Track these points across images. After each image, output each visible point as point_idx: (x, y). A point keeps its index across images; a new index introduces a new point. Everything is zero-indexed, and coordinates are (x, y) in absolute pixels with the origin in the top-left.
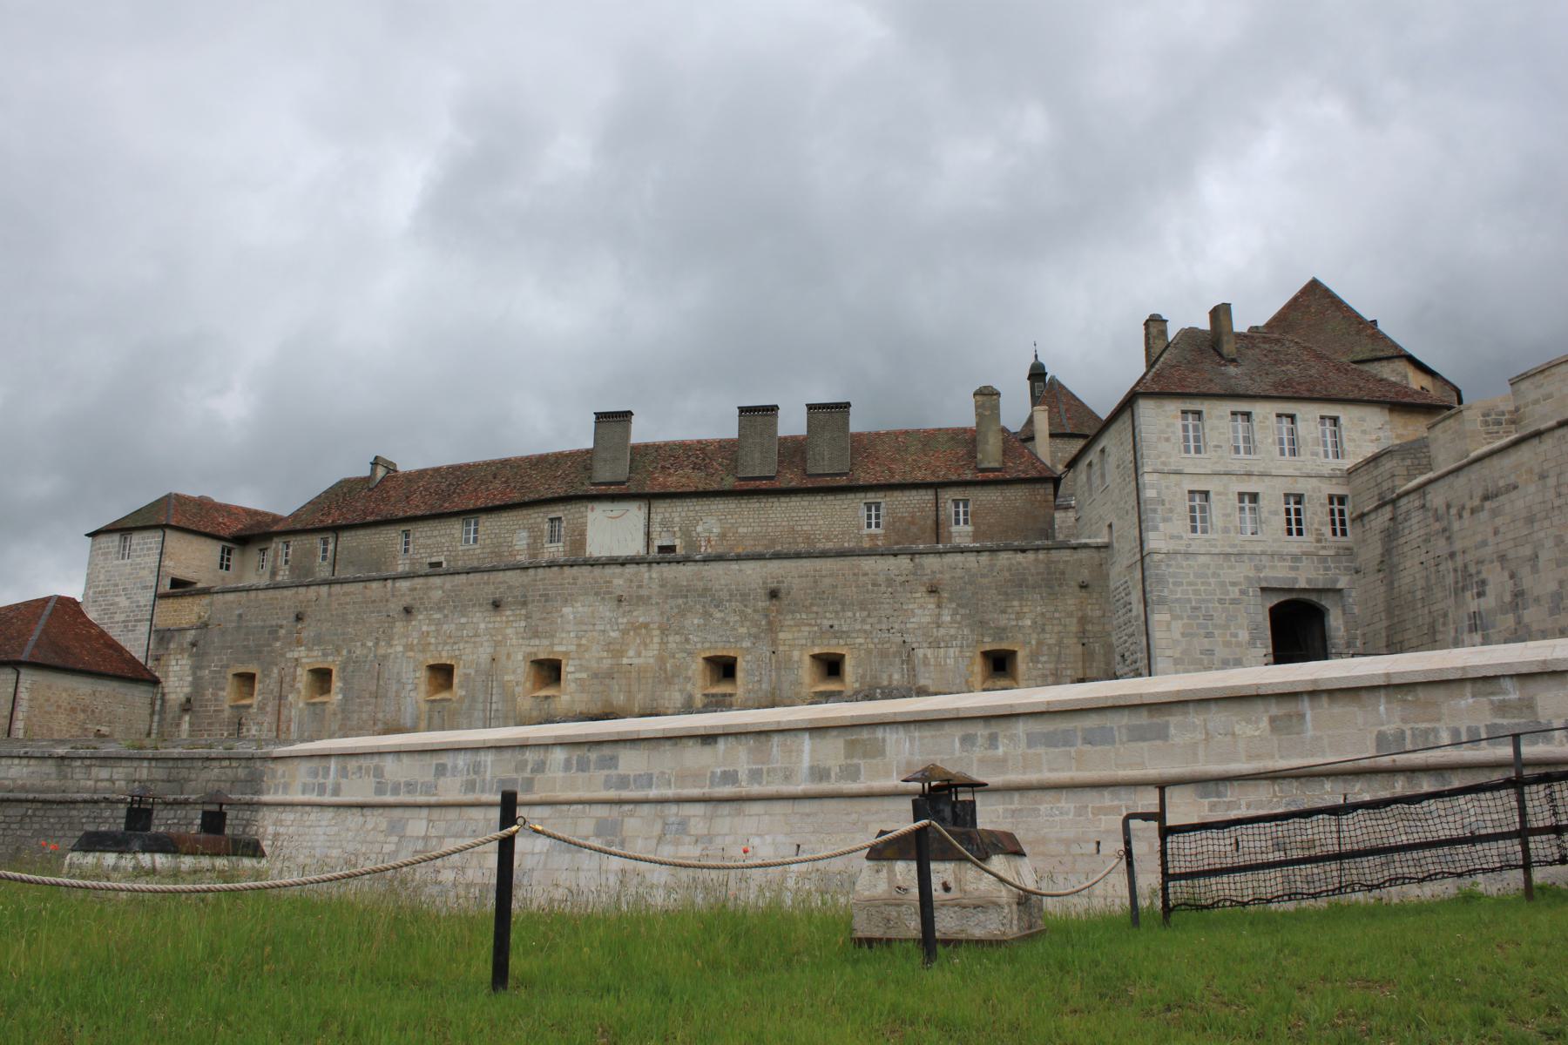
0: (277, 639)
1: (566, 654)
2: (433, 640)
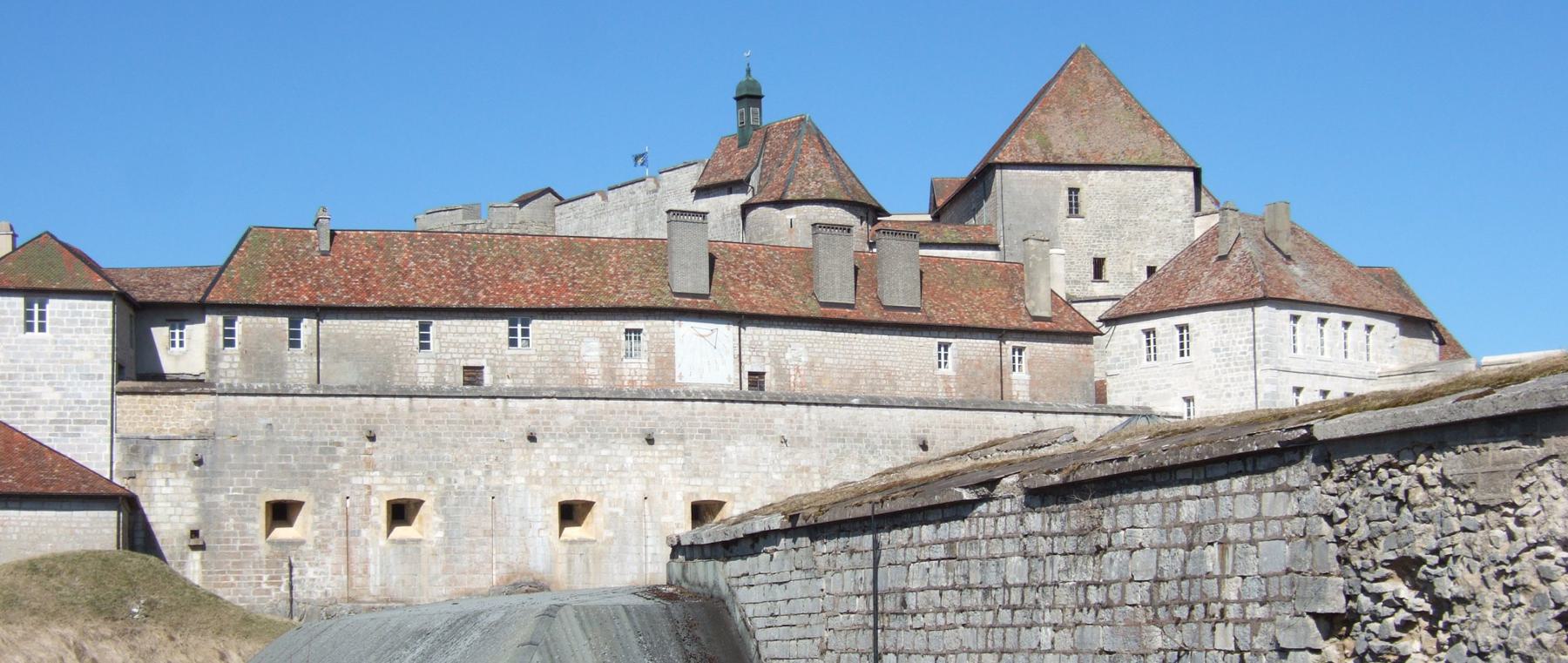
0: (335, 460)
1: (732, 496)
2: (566, 473)
